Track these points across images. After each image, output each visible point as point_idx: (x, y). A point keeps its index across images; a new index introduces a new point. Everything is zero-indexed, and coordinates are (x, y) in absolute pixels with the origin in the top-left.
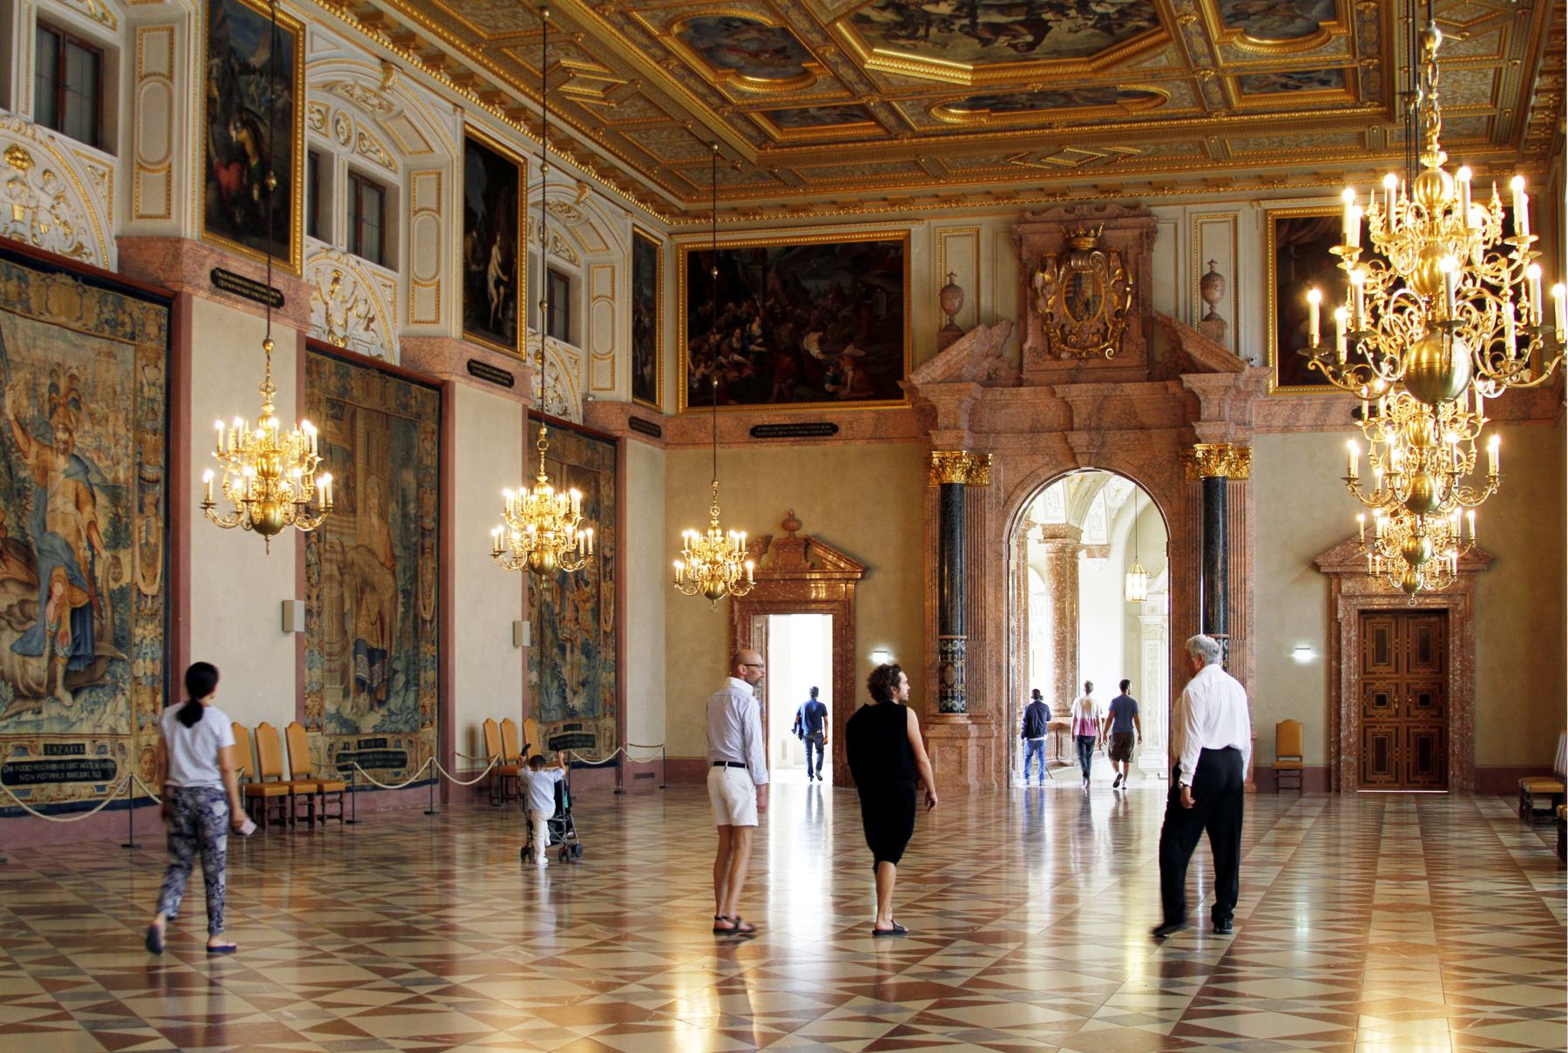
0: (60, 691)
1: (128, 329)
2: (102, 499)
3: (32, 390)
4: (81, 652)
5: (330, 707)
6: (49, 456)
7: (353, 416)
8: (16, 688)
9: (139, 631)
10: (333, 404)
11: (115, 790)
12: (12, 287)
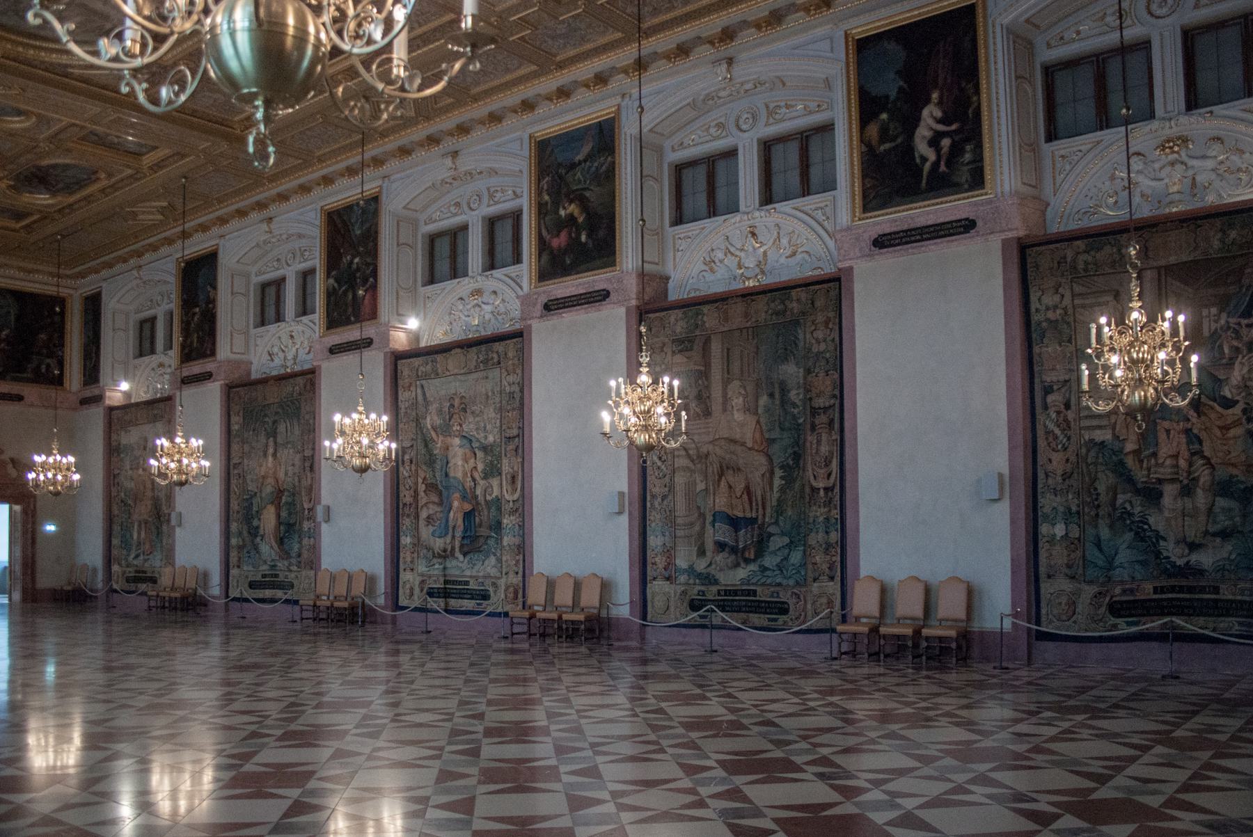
0: (458, 554)
2: (480, 454)
3: (440, 412)
5: (682, 563)
7: (707, 341)
9: (505, 521)
10: (679, 341)
12: (429, 367)
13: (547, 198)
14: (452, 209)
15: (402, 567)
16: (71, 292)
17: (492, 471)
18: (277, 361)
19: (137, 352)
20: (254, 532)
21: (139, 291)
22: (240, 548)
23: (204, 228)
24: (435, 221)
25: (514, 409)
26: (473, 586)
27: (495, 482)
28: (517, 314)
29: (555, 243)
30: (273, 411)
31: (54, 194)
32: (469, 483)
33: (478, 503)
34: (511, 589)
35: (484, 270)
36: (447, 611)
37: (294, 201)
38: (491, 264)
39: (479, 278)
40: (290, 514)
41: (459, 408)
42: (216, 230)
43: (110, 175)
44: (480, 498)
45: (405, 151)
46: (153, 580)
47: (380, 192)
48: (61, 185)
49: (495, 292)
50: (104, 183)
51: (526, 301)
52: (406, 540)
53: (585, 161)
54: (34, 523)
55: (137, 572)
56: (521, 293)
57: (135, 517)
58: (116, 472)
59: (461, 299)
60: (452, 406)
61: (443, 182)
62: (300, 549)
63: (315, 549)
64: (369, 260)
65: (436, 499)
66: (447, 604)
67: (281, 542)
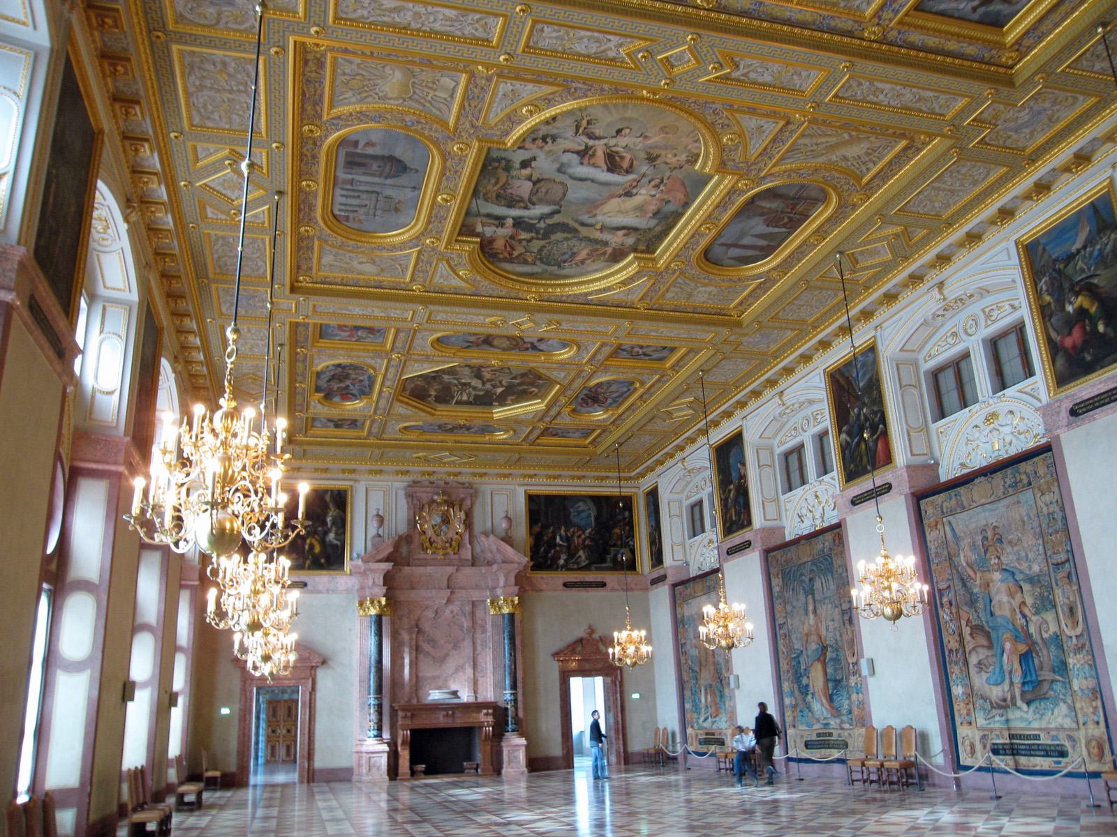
0: (1019, 703)
1: (1025, 481)
2: (1026, 587)
3: (973, 546)
4: (1028, 679)
6: (988, 575)
8: (991, 703)
11: (1069, 764)
12: (953, 502)
13: (1048, 298)
14: (949, 340)
15: (958, 720)
16: (634, 490)
17: (1046, 603)
18: (808, 522)
19: (692, 534)
20: (804, 690)
21: (685, 480)
22: (794, 707)
23: (728, 414)
24: (935, 356)
25: (1057, 532)
26: (1044, 740)
27: (1049, 616)
28: (1041, 430)
29: (1068, 342)
30: (807, 570)
31: (606, 411)
32: (1020, 621)
33: (1034, 643)
34: (1094, 743)
35: (995, 392)
36: (1017, 770)
37: (800, 372)
38: (1001, 382)
39: (991, 401)
40: (835, 670)
41: (993, 540)
42: (739, 414)
43: (642, 384)
44: (1036, 637)
45: (890, 298)
46: (721, 743)
47: (875, 342)
48: (609, 401)
49: (1011, 412)
50: (641, 391)
51: (1047, 412)
52: (958, 690)
53: (1084, 247)
54: (622, 693)
55: (707, 734)
56: (1038, 404)
57: (702, 682)
58: (683, 641)
59: (976, 426)
60: (985, 538)
61: (935, 316)
62: (850, 705)
63: (863, 706)
64: (875, 408)
65: (985, 643)
66: (1016, 763)
67: (831, 699)
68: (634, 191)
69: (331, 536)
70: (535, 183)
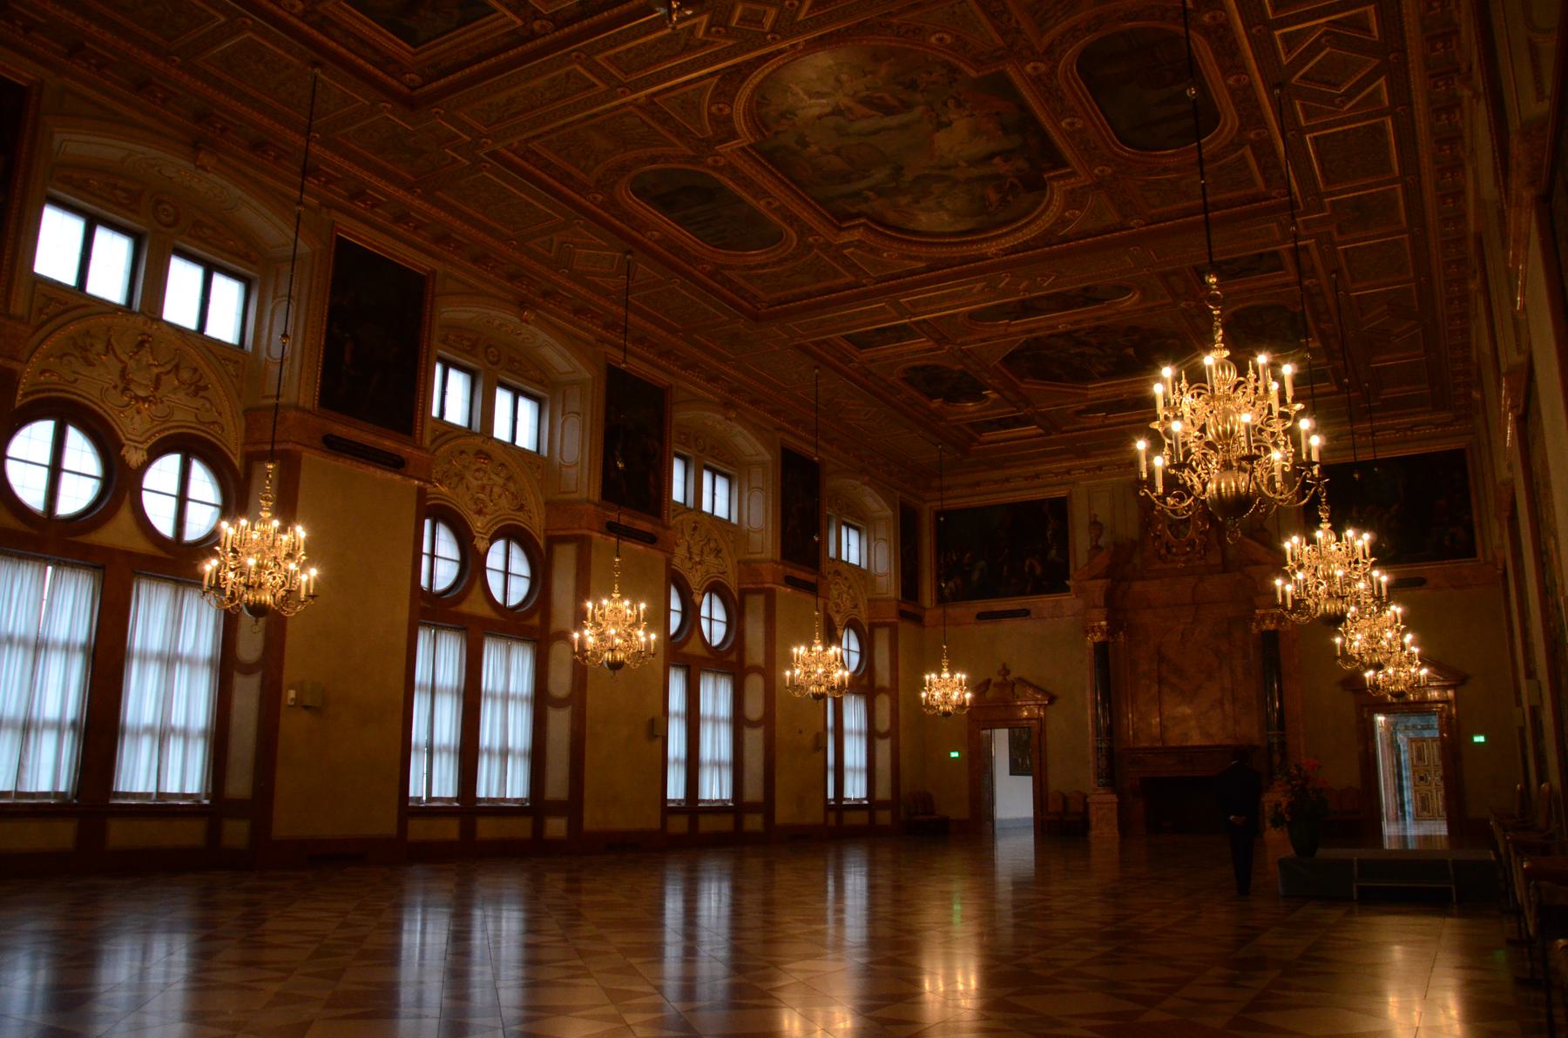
68: (944, 119)
69: (1053, 553)
70: (837, 152)
